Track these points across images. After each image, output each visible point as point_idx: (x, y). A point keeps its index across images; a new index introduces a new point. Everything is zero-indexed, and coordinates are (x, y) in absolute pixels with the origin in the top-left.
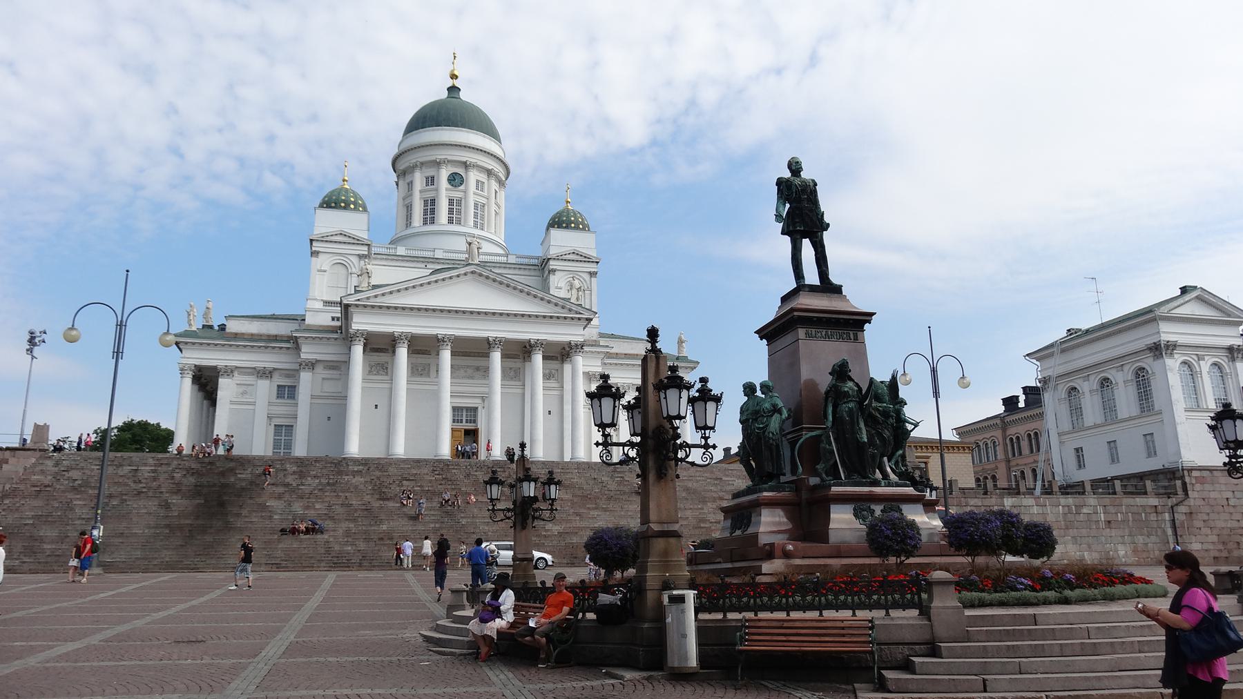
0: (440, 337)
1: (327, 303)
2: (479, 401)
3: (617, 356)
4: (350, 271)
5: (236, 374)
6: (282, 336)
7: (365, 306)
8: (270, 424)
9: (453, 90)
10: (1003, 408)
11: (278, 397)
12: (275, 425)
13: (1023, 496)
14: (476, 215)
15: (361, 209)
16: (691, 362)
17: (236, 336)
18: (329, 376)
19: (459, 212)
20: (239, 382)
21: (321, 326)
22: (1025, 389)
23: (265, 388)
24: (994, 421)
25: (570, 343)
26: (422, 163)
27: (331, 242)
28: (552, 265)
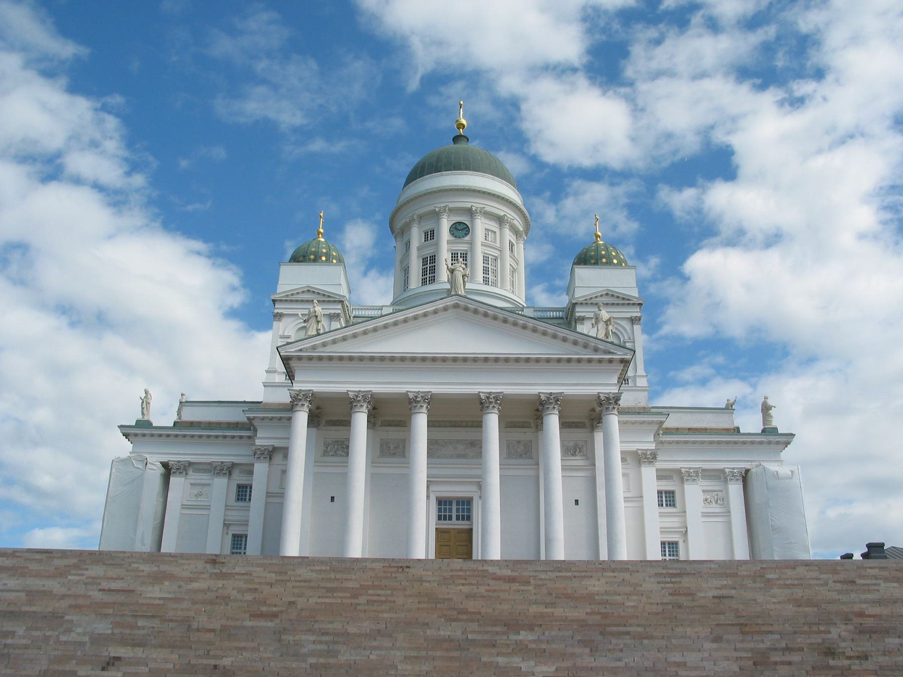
0: (411, 396)
3: (677, 431)
5: (190, 472)
7: (310, 358)
8: (227, 533)
11: (238, 500)
12: (234, 536)
14: (486, 271)
15: (334, 261)
17: (192, 425)
20: (193, 481)
21: (280, 404)
23: (221, 487)
25: (599, 397)
27: (297, 301)
28: (578, 312)
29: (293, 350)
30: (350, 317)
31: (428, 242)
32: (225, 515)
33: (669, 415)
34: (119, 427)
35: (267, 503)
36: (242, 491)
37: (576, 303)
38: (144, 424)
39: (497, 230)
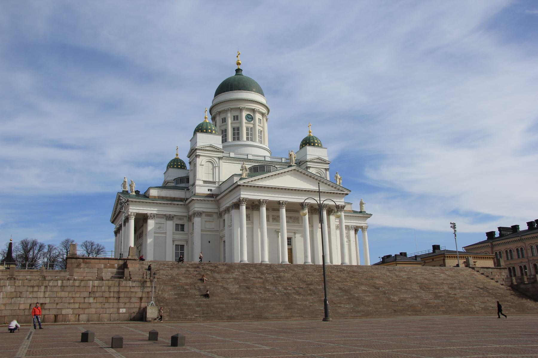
1: (205, 182)
2: (293, 234)
4: (214, 166)
6: (177, 198)
7: (247, 186)
8: (173, 244)
9: (238, 71)
10: (487, 237)
12: (176, 245)
16: (367, 214)
18: (208, 220)
19: (252, 135)
22: (500, 229)
23: (170, 225)
24: (486, 244)
26: (232, 109)
28: (308, 164)
29: (242, 182)
31: (234, 121)
35: (202, 234)
36: (177, 227)
37: (307, 161)
39: (261, 118)
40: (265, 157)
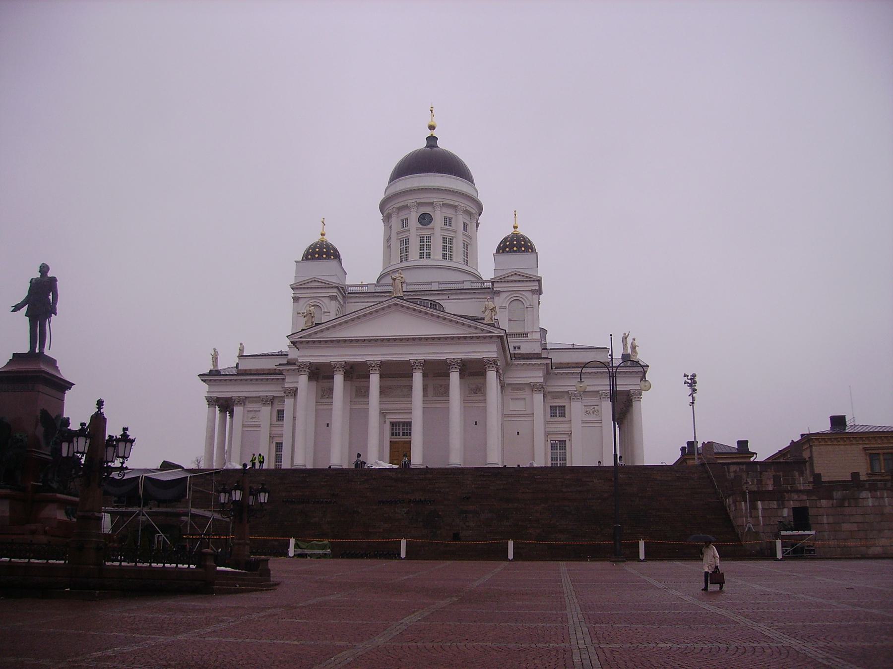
0: (369, 363)
5: (247, 403)
7: (308, 342)
8: (272, 442)
9: (432, 140)
11: (278, 420)
12: (276, 443)
13: (856, 489)
14: (444, 248)
19: (429, 247)
20: (249, 409)
23: (266, 413)
28: (496, 287)
30: (345, 294)
31: (403, 229)
32: (270, 431)
33: (551, 359)
34: (199, 375)
38: (215, 373)
40: (430, 283)
